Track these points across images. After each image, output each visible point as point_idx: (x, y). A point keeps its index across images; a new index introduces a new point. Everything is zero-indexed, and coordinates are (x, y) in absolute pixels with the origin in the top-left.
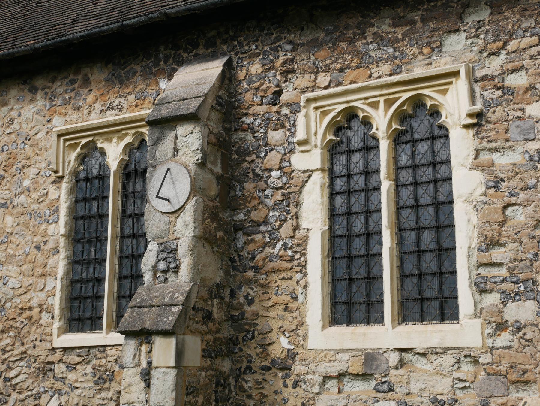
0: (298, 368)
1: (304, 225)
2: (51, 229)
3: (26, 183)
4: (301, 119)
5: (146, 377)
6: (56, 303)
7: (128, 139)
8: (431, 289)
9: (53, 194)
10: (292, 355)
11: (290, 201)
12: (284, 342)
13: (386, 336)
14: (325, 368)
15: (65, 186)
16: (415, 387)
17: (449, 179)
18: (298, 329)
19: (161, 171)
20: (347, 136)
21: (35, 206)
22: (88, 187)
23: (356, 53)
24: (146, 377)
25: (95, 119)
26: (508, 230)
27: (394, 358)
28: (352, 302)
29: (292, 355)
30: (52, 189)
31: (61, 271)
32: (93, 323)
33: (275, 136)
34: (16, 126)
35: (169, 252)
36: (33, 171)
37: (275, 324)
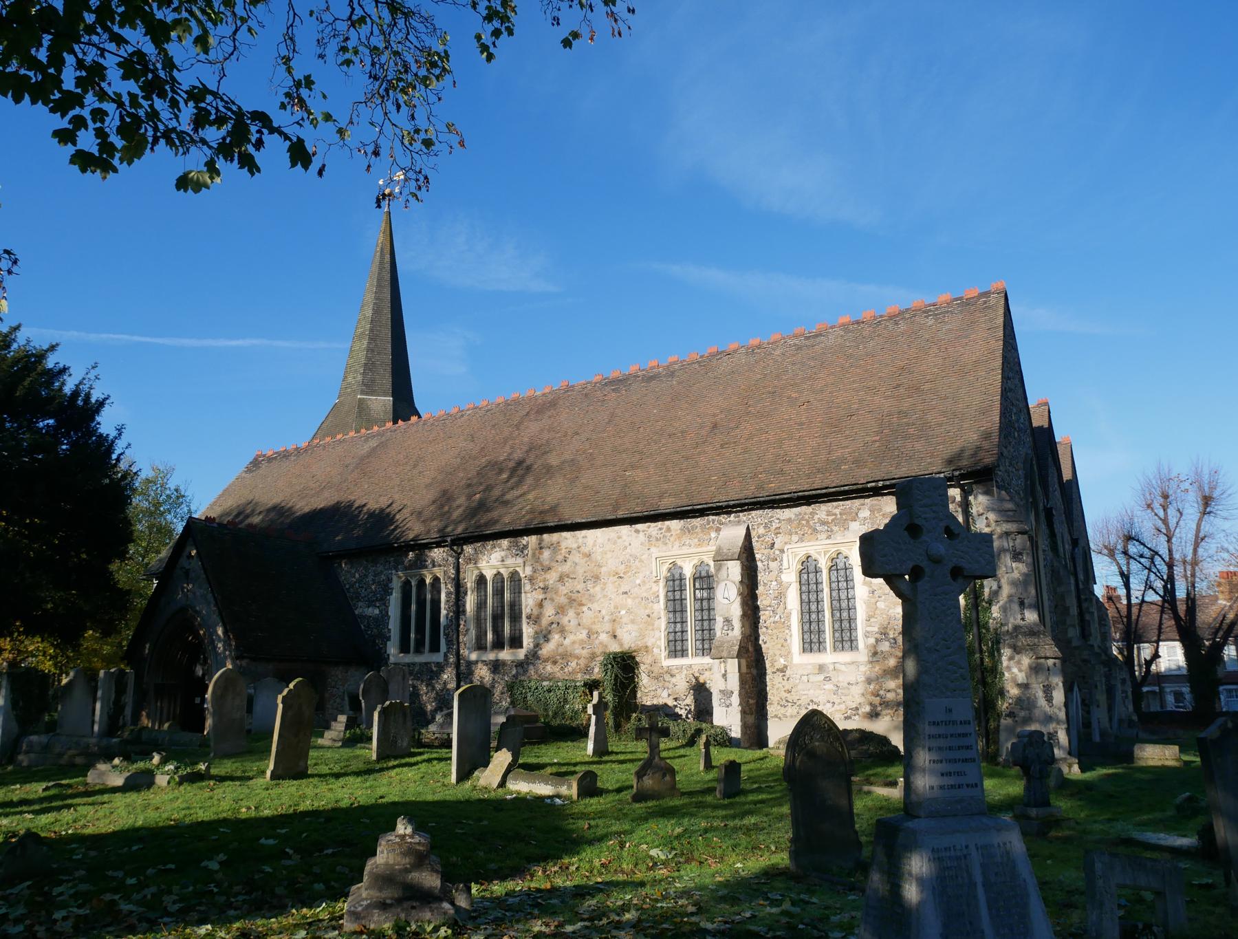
0: (788, 673)
1: (789, 607)
2: (655, 606)
3: (638, 582)
4: (785, 556)
5: (724, 676)
6: (663, 643)
7: (695, 561)
8: (846, 636)
9: (655, 588)
10: (786, 667)
11: (781, 596)
12: (782, 661)
13: (828, 657)
14: (800, 672)
15: (662, 583)
16: (841, 679)
17: (853, 588)
18: (788, 654)
19: (723, 584)
20: (808, 569)
21: (645, 595)
22: (675, 582)
23: (810, 527)
24: (724, 676)
25: (676, 551)
26: (878, 612)
27: (831, 667)
28: (812, 643)
29: (786, 667)
30: (654, 585)
31: (663, 626)
32: (684, 653)
33: (773, 565)
34: (628, 550)
35: (728, 621)
36: (641, 575)
37: (778, 653)
